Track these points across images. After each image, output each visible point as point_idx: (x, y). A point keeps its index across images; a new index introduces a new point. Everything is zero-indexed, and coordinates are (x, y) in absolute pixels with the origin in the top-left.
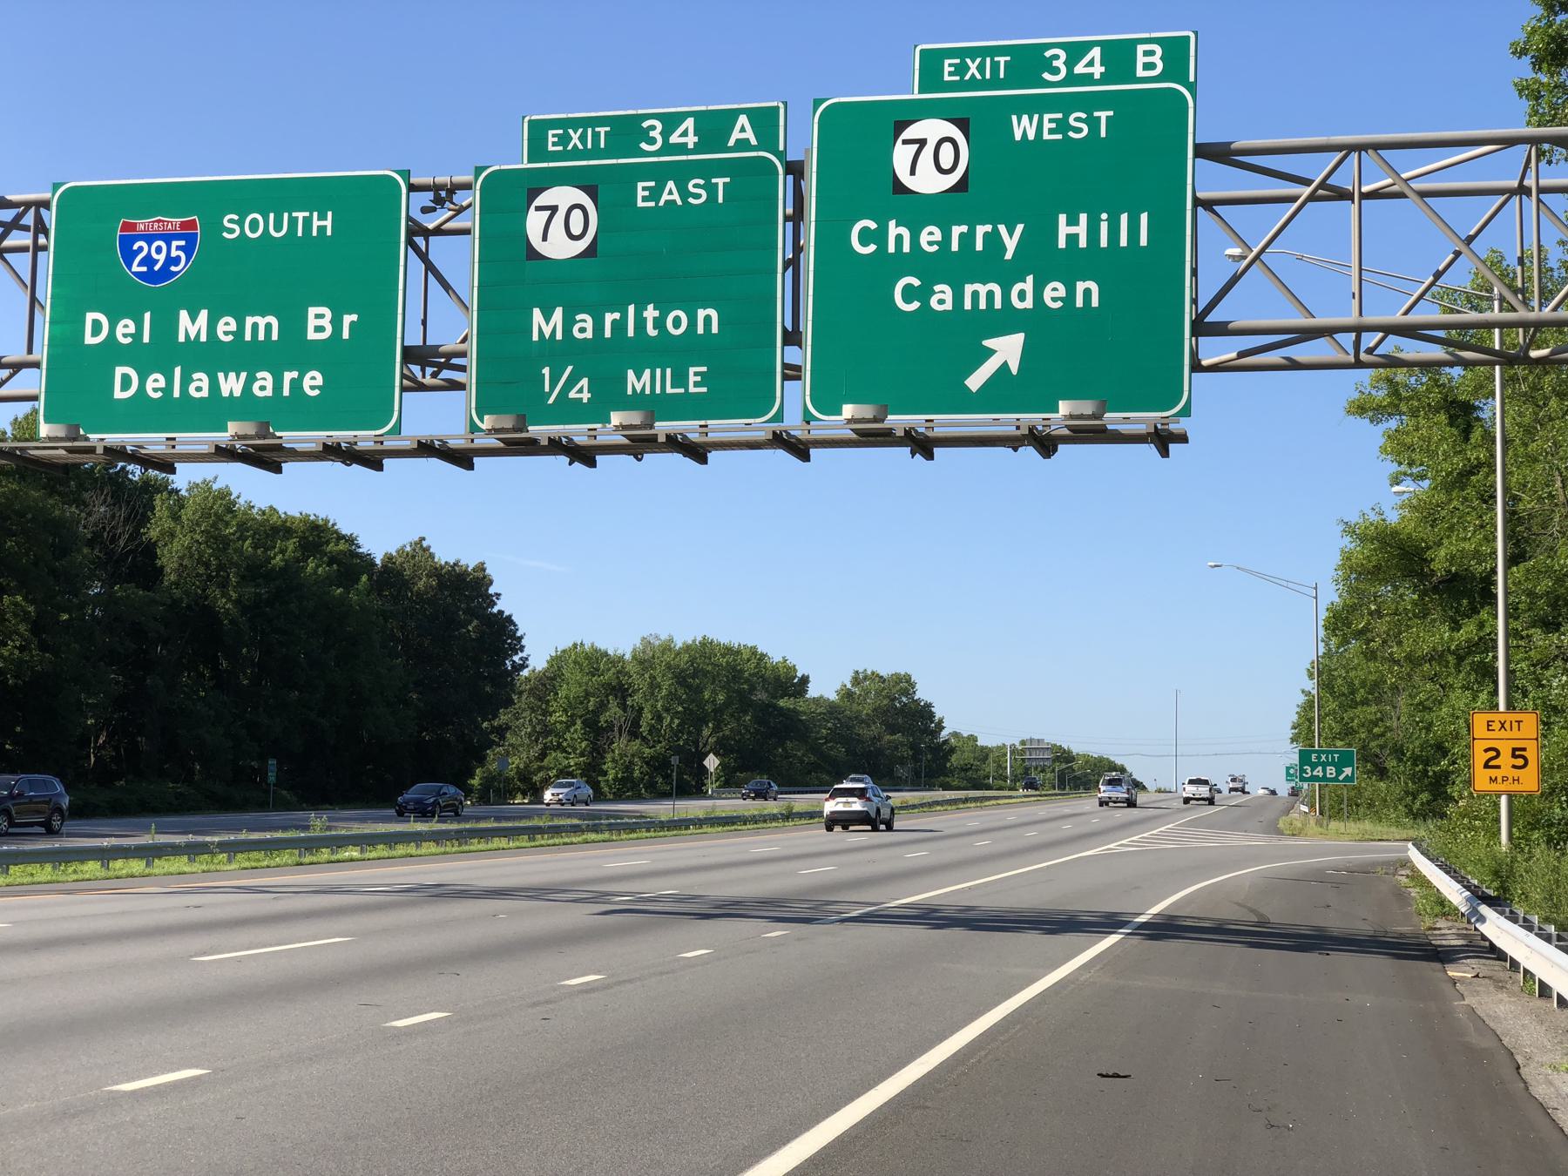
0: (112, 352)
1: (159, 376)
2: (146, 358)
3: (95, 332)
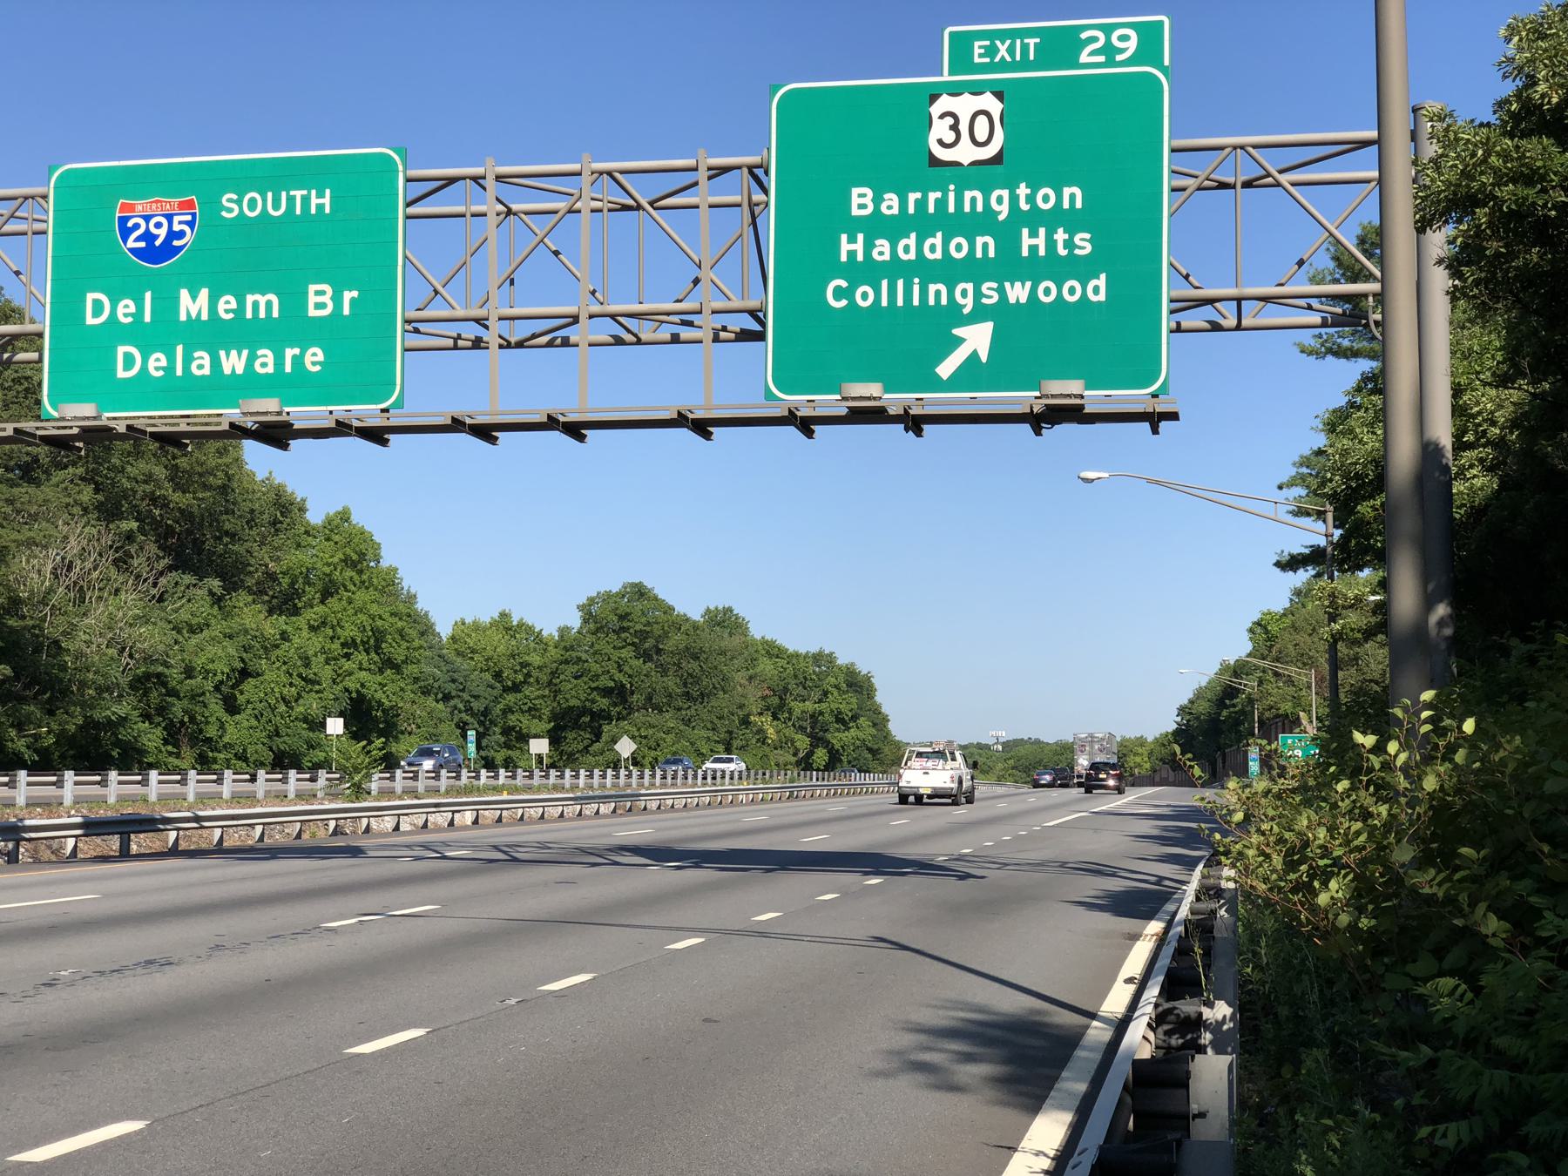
2: (147, 337)
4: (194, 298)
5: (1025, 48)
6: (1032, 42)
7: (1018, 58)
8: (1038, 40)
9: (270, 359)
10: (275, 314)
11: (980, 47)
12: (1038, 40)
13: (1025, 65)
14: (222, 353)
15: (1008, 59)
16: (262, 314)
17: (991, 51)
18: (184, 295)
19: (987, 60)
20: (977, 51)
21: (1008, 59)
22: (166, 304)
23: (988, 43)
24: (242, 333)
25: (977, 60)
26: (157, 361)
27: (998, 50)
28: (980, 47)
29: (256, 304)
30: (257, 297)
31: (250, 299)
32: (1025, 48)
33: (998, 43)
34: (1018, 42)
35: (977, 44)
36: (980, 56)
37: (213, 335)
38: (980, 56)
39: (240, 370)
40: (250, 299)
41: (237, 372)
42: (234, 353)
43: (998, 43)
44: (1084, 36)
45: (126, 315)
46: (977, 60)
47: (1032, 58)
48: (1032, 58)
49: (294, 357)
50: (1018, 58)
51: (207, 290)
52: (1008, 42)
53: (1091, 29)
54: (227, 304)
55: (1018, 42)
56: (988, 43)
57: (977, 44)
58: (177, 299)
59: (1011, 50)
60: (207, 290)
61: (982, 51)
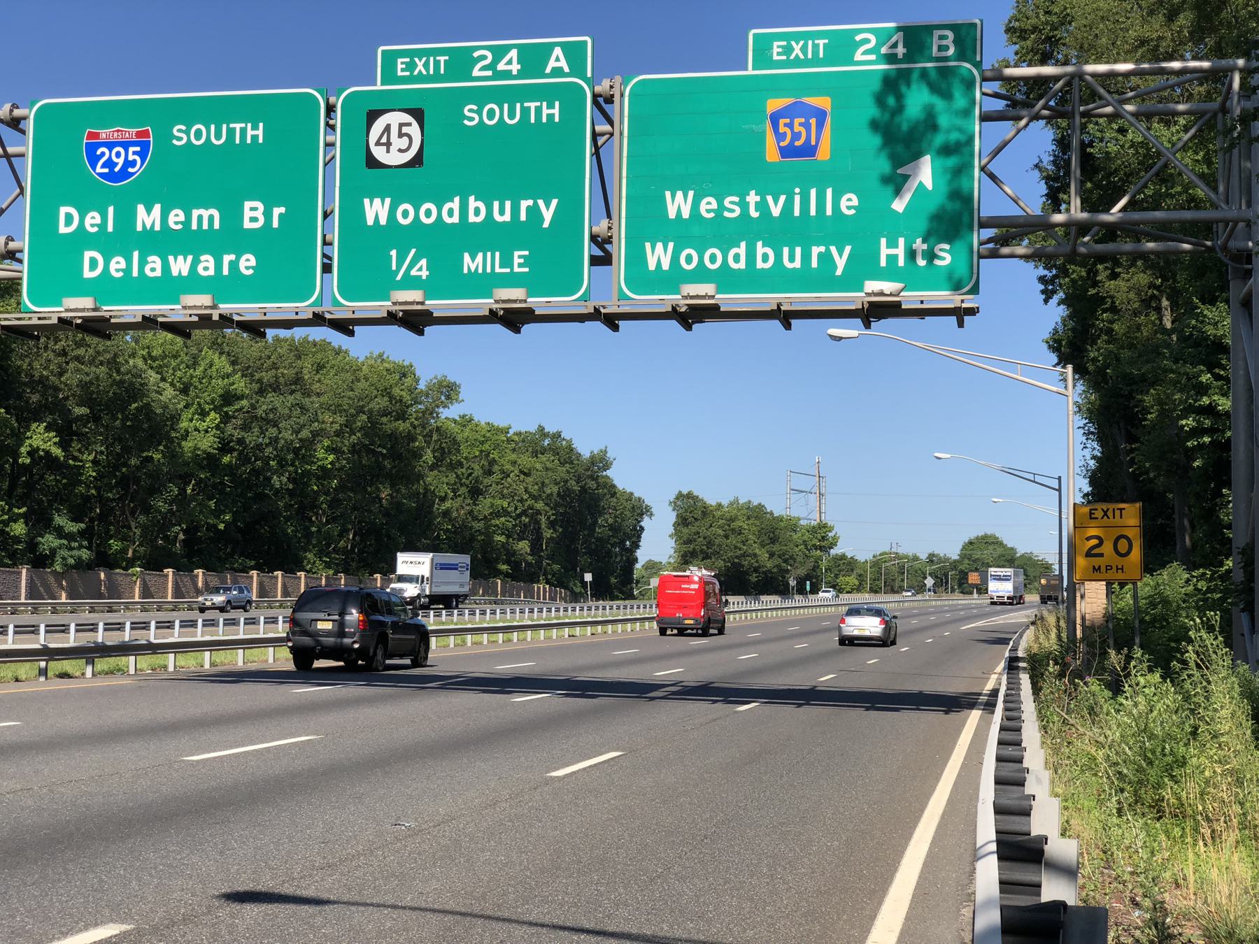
0: (81, 239)
2: (109, 244)
4: (149, 211)
7: (810, 56)
10: (217, 226)
14: (171, 258)
15: (802, 57)
16: (205, 226)
17: (788, 50)
18: (141, 209)
24: (190, 242)
26: (117, 264)
33: (793, 43)
37: (163, 242)
39: (185, 273)
41: (183, 274)
42: (180, 258)
43: (793, 43)
48: (821, 55)
49: (231, 262)
50: (810, 56)
51: (159, 205)
52: (802, 43)
60: (159, 205)
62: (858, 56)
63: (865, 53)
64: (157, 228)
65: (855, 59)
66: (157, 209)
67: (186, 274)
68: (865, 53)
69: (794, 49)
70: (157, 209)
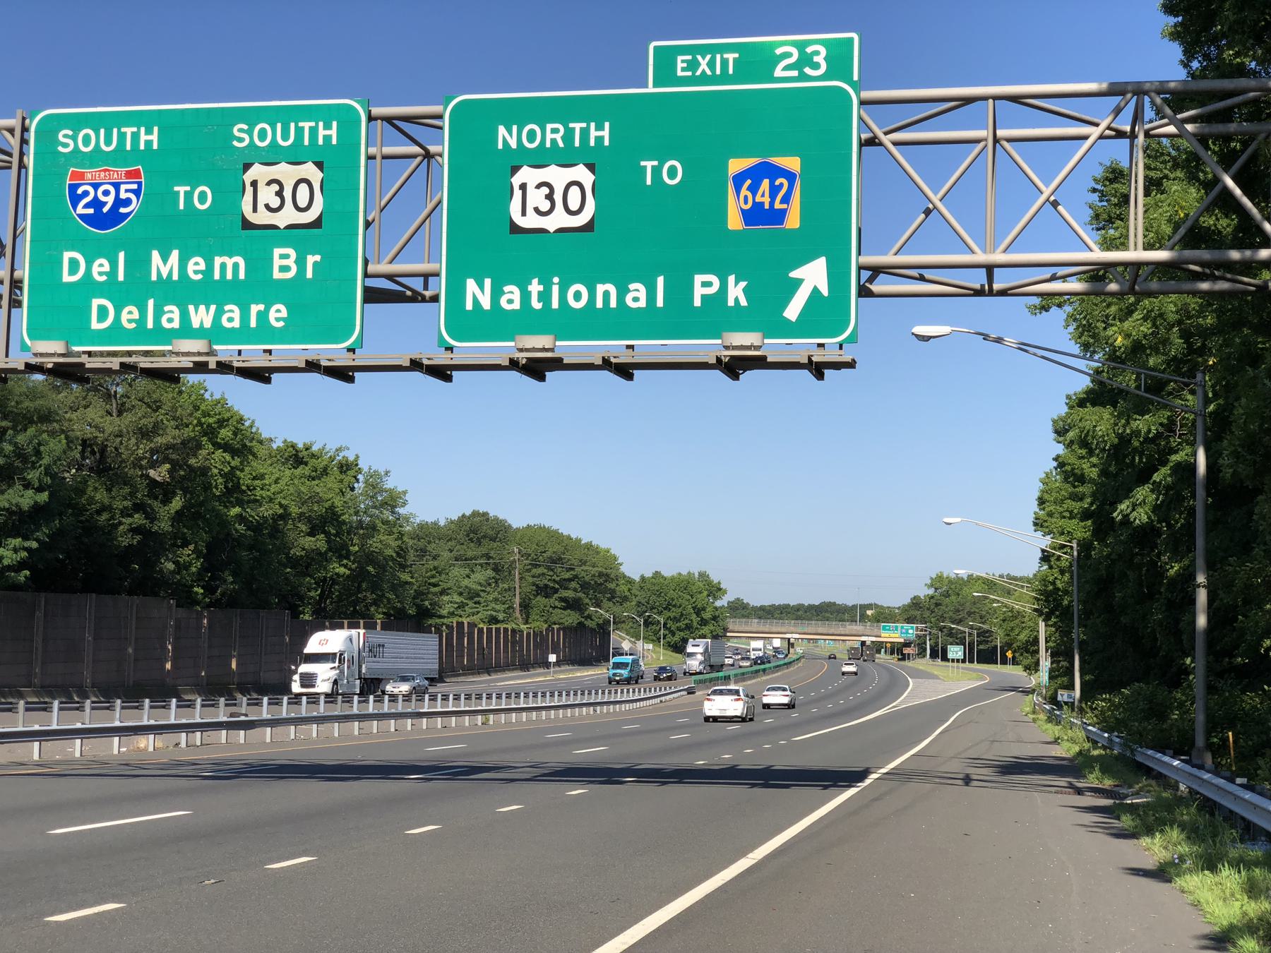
0: (88, 287)
1: (134, 309)
2: (121, 293)
3: (73, 270)
4: (165, 259)
5: (725, 63)
6: (731, 57)
7: (718, 72)
8: (737, 55)
9: (236, 315)
11: (683, 61)
12: (737, 55)
13: (724, 78)
14: (191, 308)
15: (709, 73)
19: (689, 73)
20: (680, 65)
21: (709, 73)
22: (138, 264)
23: (689, 57)
25: (680, 73)
26: (129, 315)
27: (699, 64)
28: (683, 61)
29: (223, 266)
30: (225, 259)
31: (218, 261)
32: (725, 63)
34: (718, 56)
35: (680, 58)
36: (683, 69)
38: (683, 69)
40: (218, 261)
42: (202, 308)
44: (779, 51)
45: (100, 274)
46: (680, 73)
47: (731, 72)
48: (731, 72)
50: (718, 72)
51: (177, 251)
52: (708, 57)
53: (785, 45)
54: (196, 266)
55: (718, 56)
56: (689, 57)
57: (680, 58)
58: (148, 261)
59: (711, 64)
60: (177, 251)
61: (685, 65)
62: (778, 72)
63: (786, 68)
64: (175, 277)
65: (775, 75)
66: (175, 256)
67: (209, 326)
68: (786, 68)
69: (707, 64)
70: (175, 255)
